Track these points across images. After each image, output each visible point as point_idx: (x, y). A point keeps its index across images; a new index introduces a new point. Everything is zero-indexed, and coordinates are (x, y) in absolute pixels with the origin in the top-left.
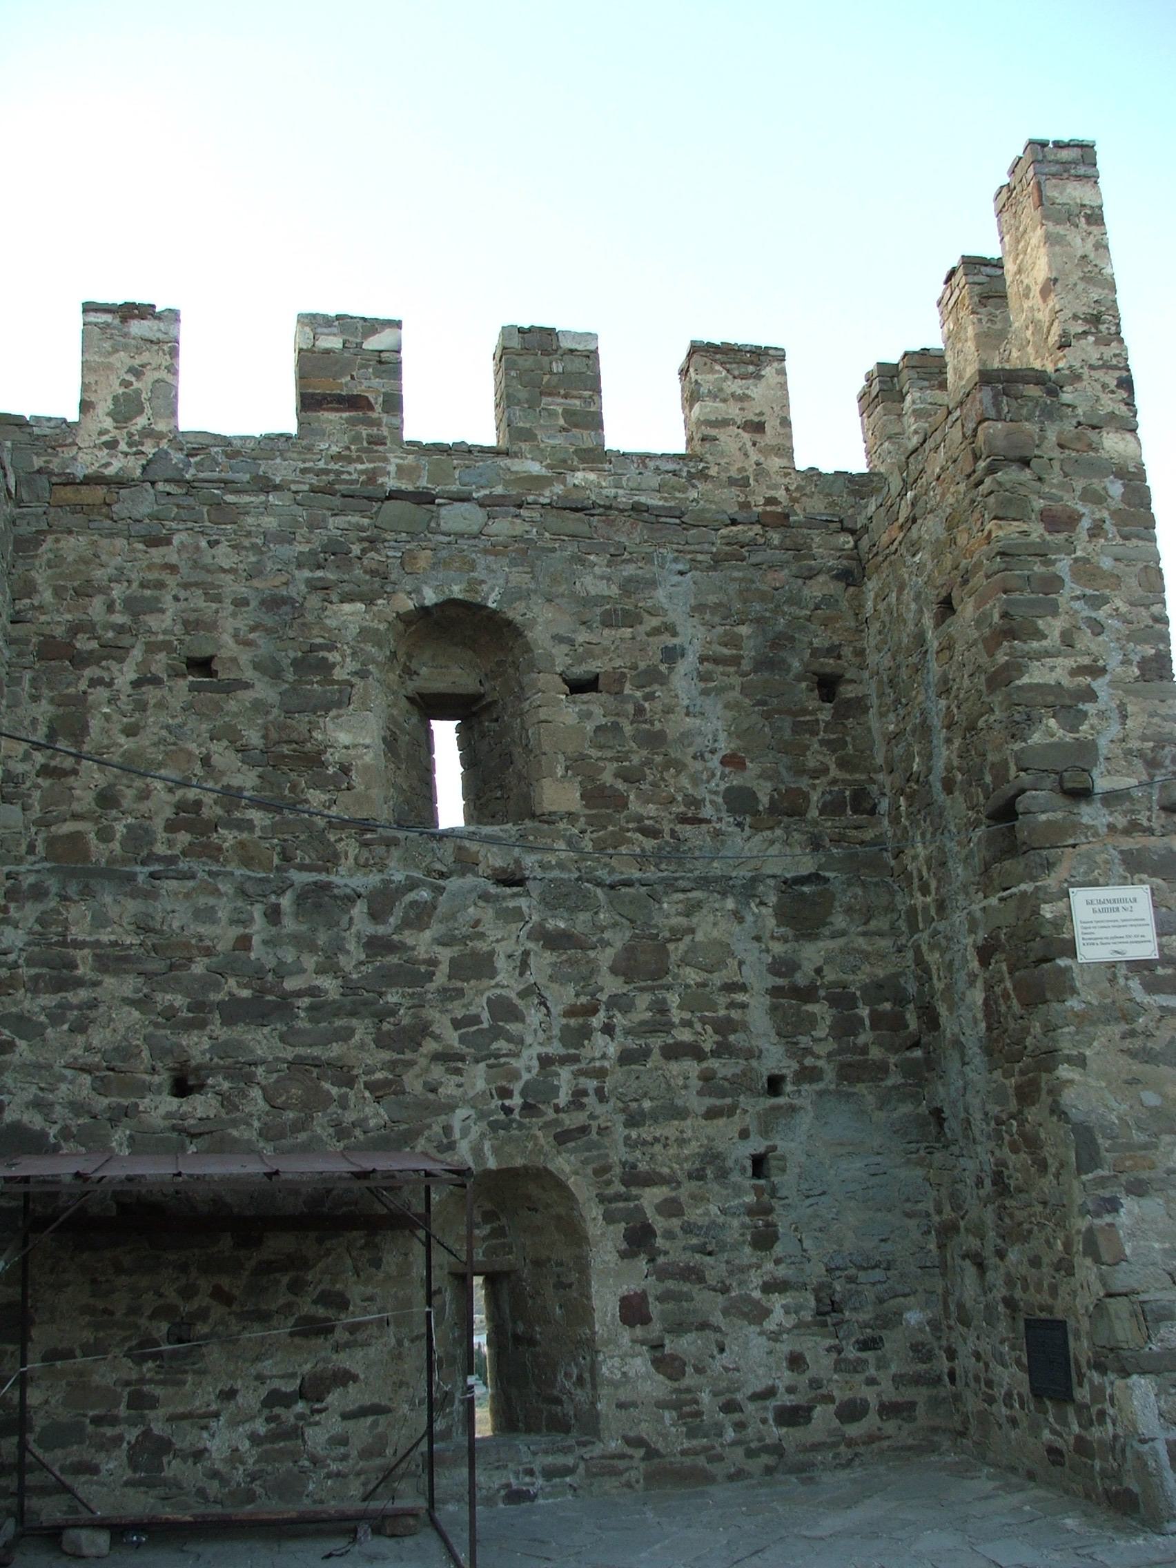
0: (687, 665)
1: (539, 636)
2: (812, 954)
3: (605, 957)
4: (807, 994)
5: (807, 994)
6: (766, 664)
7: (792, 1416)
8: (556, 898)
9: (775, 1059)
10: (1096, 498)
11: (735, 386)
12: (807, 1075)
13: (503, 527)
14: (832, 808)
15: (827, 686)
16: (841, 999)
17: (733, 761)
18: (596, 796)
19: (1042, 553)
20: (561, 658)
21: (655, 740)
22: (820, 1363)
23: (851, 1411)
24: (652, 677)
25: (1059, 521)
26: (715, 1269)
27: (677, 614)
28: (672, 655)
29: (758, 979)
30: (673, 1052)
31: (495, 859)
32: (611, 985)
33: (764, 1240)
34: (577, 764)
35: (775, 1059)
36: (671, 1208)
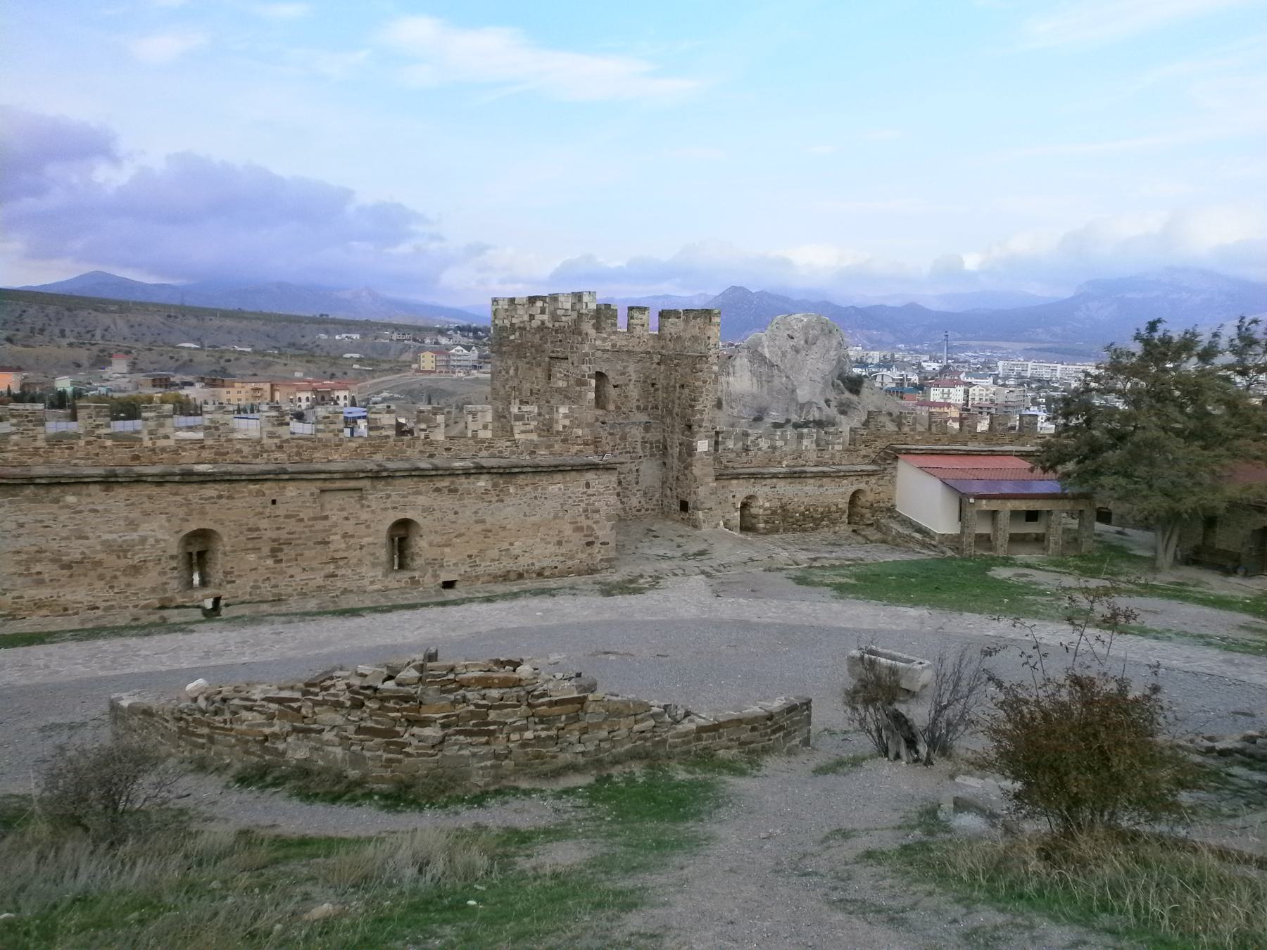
0: (633, 382)
1: (610, 378)
2: (648, 435)
3: (618, 437)
4: (646, 442)
5: (646, 442)
6: (645, 382)
7: (639, 511)
8: (613, 426)
9: (641, 454)
10: (710, 378)
11: (640, 316)
12: (645, 456)
13: (606, 356)
14: (652, 408)
15: (653, 385)
16: (651, 443)
17: (638, 400)
18: (618, 408)
19: (701, 387)
20: (613, 382)
21: (626, 397)
22: (643, 503)
23: (647, 510)
24: (627, 385)
25: (705, 382)
26: (630, 487)
27: (632, 373)
28: (630, 380)
29: (640, 440)
30: (626, 453)
31: (601, 419)
32: (618, 441)
33: (637, 483)
34: (615, 401)
35: (641, 454)
36: (624, 478)
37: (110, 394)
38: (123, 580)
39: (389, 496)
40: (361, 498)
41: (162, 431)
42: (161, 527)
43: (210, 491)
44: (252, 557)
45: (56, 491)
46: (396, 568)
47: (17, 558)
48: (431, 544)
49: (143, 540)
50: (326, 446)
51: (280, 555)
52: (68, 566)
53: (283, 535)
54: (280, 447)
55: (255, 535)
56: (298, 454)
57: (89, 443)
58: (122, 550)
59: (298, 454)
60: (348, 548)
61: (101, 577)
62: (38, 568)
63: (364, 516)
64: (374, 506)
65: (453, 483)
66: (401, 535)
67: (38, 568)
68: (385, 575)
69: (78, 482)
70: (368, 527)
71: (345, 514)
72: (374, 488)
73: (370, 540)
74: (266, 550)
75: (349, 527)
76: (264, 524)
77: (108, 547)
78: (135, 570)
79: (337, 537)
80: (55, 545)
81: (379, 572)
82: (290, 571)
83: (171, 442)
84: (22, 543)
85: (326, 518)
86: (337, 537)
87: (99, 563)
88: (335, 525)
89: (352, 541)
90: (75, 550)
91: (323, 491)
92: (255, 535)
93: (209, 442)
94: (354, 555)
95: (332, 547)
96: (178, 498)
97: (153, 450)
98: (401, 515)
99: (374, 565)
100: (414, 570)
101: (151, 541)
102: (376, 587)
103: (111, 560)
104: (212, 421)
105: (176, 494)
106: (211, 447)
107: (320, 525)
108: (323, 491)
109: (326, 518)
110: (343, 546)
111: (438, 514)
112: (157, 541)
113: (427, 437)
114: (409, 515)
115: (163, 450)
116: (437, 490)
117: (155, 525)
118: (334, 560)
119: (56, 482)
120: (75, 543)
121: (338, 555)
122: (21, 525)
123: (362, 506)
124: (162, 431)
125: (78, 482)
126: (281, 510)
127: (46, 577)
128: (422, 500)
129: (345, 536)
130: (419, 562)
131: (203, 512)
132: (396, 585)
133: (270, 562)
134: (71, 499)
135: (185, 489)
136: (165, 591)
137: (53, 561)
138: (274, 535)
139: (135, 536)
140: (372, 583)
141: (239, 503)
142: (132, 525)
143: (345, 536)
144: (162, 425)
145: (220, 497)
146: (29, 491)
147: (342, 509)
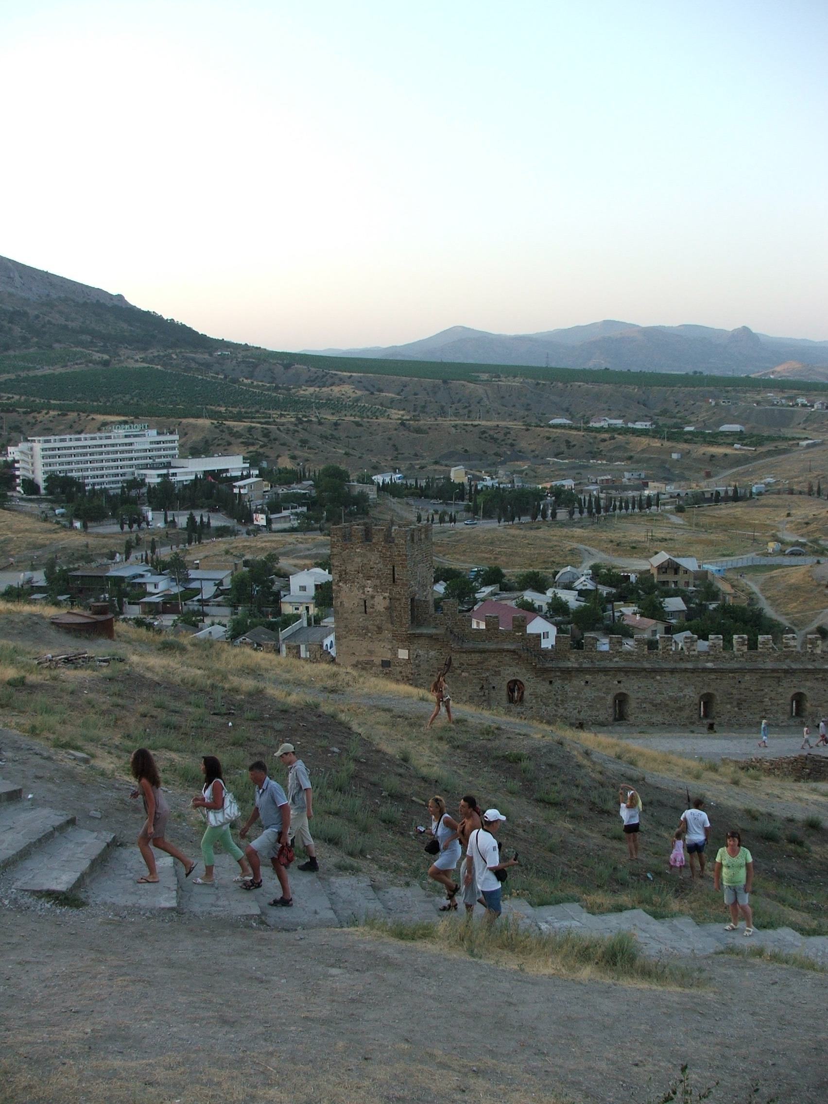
37: (501, 486)
38: (676, 713)
39: (792, 681)
40: (779, 681)
41: (693, 648)
42: (692, 691)
43: (713, 677)
44: (729, 706)
45: (653, 674)
46: (794, 714)
47: (637, 701)
48: (811, 705)
49: (685, 696)
50: (763, 655)
51: (741, 706)
52: (655, 705)
53: (743, 697)
54: (742, 656)
55: (731, 696)
56: (750, 659)
57: (663, 653)
58: (675, 700)
59: (750, 659)
60: (772, 705)
61: (667, 711)
62: (644, 705)
63: (780, 690)
64: (785, 685)
65: (824, 676)
66: (799, 698)
67: (644, 705)
68: (789, 719)
69: (661, 671)
70: (782, 695)
71: (771, 689)
72: (785, 677)
73: (782, 701)
74: (735, 704)
75: (773, 694)
76: (735, 691)
77: (671, 698)
78: (681, 709)
79: (767, 699)
80: (651, 697)
81: (786, 717)
82: (745, 714)
83: (696, 653)
84: (639, 695)
85: (762, 690)
86: (767, 699)
87: (667, 705)
88: (766, 694)
89: (774, 701)
90: (659, 699)
91: (762, 677)
92: (731, 696)
93: (712, 653)
94: (775, 708)
95: (765, 704)
96: (700, 679)
97: (688, 656)
98: (797, 690)
99: (784, 714)
100: (803, 717)
101: (688, 697)
102: (783, 724)
103: (672, 704)
104: (713, 643)
105: (699, 677)
106: (712, 655)
107: (759, 693)
108: (762, 677)
109: (762, 690)
110: (770, 704)
111: (816, 691)
112: (690, 697)
113: (812, 651)
114: (801, 691)
115: (693, 656)
116: (817, 679)
117: (689, 690)
118: (765, 710)
119: (654, 671)
120: (659, 696)
121: (768, 708)
122: (639, 688)
123: (779, 685)
124: (693, 648)
125: (661, 671)
126: (743, 686)
127: (647, 709)
128: (808, 684)
129: (771, 699)
130: (807, 713)
131: (709, 685)
132: (794, 724)
133: (736, 709)
134: (658, 678)
135: (702, 675)
136: (692, 719)
137: (650, 703)
138: (739, 697)
139: (681, 694)
140: (782, 722)
141: (725, 682)
142: (681, 689)
143: (771, 699)
144: (693, 645)
145: (717, 679)
146: (643, 673)
147: (769, 686)
